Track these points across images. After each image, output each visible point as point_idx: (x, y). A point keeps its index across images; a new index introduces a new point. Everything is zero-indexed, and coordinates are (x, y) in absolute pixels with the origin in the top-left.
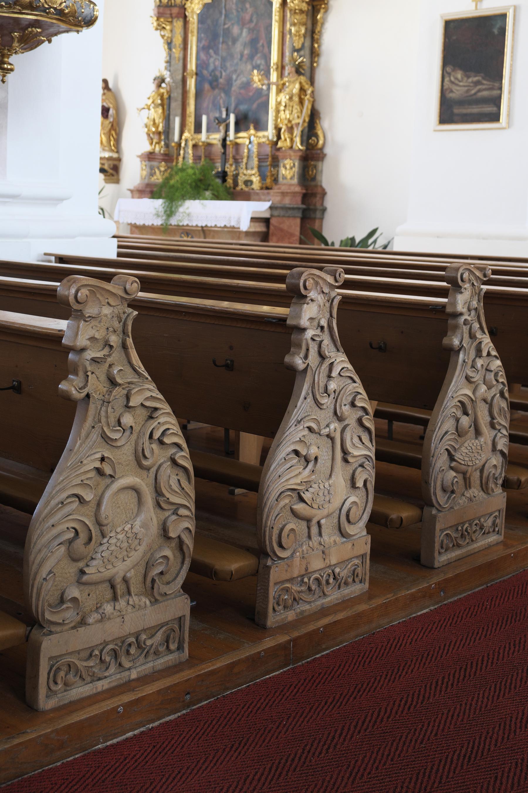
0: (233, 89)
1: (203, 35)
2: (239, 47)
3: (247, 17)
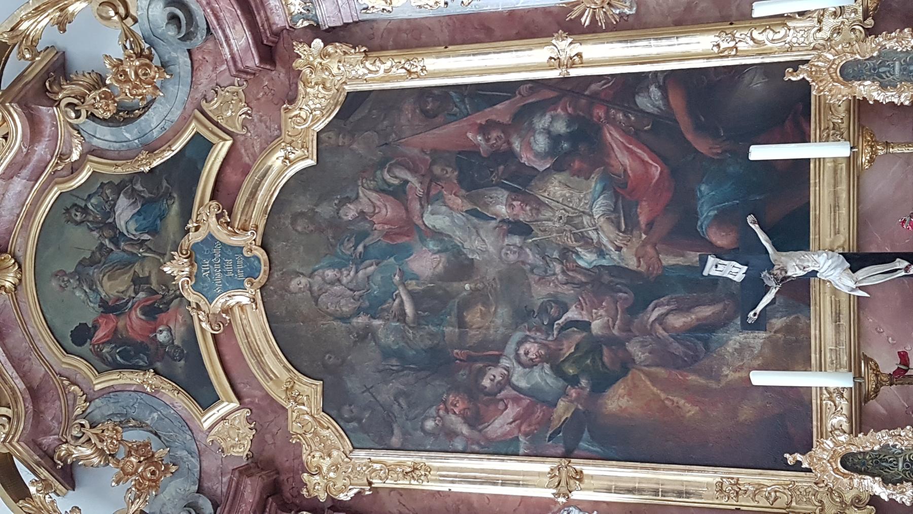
0: (632, 263)
1: (430, 424)
2: (483, 245)
3: (388, 210)
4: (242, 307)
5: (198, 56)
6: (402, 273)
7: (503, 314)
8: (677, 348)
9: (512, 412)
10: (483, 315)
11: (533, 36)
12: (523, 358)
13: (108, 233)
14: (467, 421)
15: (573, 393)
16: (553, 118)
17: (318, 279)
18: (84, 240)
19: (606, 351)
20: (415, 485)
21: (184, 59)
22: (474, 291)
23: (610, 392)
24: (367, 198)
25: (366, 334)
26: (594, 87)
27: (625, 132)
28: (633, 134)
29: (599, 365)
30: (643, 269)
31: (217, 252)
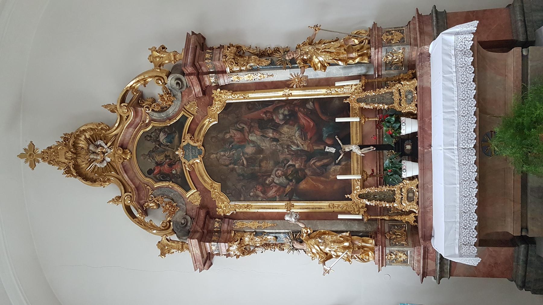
0: (306, 149)
1: (252, 194)
2: (266, 145)
3: (238, 135)
4: (197, 163)
5: (183, 93)
6: (243, 153)
7: (272, 163)
8: (318, 171)
9: (274, 189)
10: (266, 163)
11: (278, 88)
12: (277, 175)
13: (157, 143)
14: (262, 192)
15: (291, 184)
16: (284, 110)
17: (219, 155)
18: (151, 145)
19: (299, 172)
20: (248, 210)
21: (180, 94)
22: (264, 157)
23: (301, 183)
24: (233, 132)
25: (233, 170)
26: (295, 102)
27: (304, 114)
28: (306, 115)
29: (298, 176)
30: (309, 150)
31: (190, 148)
